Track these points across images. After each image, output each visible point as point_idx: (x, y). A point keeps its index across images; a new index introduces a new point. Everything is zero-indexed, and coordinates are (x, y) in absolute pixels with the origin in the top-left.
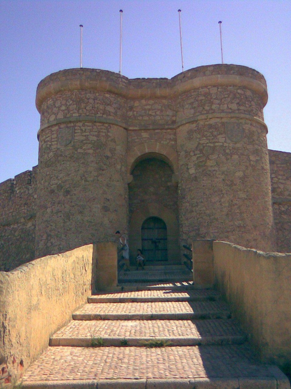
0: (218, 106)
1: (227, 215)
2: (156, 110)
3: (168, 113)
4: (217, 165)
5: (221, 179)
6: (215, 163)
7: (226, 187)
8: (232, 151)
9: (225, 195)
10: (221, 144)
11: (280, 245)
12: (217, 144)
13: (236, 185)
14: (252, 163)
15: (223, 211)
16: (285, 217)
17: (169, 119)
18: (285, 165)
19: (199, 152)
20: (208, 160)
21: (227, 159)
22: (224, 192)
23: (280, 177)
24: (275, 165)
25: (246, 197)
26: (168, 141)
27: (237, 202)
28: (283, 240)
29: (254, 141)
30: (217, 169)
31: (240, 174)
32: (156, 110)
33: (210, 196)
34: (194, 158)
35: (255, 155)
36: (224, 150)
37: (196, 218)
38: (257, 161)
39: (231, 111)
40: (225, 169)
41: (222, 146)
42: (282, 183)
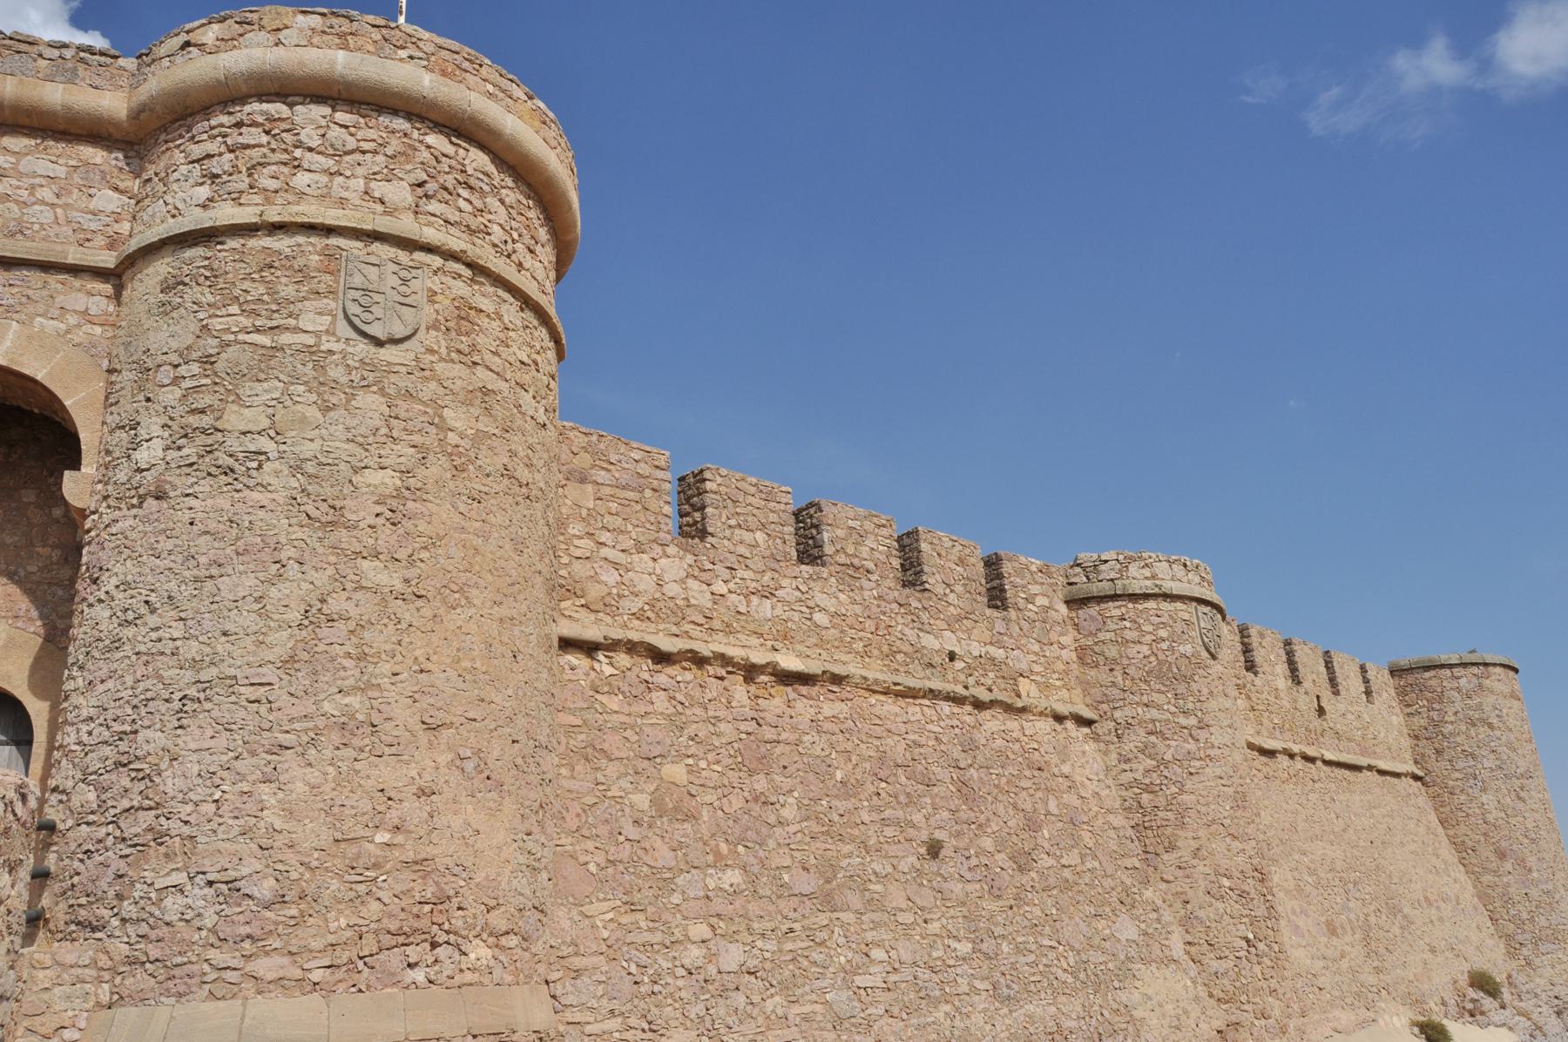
0: (324, 179)
1: (289, 663)
2: (37, 181)
3: (94, 204)
4: (276, 433)
5: (281, 497)
6: (266, 423)
7: (300, 535)
8: (355, 376)
9: (293, 569)
10: (310, 340)
11: (572, 823)
12: (285, 338)
13: (351, 527)
14: (452, 438)
15: (271, 647)
16: (613, 703)
17: (93, 226)
18: (631, 495)
19: (195, 368)
20: (235, 407)
21: (326, 409)
22: (288, 553)
23: (605, 537)
24: (589, 488)
25: (399, 586)
26: (72, 320)
27: (350, 606)
28: (590, 800)
29: (473, 347)
30: (265, 444)
31: (387, 480)
32: (37, 181)
33: (214, 571)
34: (171, 396)
35: (475, 411)
36: (320, 367)
37: (129, 680)
38: (480, 437)
39: (379, 208)
40: (308, 449)
41: (310, 350)
42: (616, 565)
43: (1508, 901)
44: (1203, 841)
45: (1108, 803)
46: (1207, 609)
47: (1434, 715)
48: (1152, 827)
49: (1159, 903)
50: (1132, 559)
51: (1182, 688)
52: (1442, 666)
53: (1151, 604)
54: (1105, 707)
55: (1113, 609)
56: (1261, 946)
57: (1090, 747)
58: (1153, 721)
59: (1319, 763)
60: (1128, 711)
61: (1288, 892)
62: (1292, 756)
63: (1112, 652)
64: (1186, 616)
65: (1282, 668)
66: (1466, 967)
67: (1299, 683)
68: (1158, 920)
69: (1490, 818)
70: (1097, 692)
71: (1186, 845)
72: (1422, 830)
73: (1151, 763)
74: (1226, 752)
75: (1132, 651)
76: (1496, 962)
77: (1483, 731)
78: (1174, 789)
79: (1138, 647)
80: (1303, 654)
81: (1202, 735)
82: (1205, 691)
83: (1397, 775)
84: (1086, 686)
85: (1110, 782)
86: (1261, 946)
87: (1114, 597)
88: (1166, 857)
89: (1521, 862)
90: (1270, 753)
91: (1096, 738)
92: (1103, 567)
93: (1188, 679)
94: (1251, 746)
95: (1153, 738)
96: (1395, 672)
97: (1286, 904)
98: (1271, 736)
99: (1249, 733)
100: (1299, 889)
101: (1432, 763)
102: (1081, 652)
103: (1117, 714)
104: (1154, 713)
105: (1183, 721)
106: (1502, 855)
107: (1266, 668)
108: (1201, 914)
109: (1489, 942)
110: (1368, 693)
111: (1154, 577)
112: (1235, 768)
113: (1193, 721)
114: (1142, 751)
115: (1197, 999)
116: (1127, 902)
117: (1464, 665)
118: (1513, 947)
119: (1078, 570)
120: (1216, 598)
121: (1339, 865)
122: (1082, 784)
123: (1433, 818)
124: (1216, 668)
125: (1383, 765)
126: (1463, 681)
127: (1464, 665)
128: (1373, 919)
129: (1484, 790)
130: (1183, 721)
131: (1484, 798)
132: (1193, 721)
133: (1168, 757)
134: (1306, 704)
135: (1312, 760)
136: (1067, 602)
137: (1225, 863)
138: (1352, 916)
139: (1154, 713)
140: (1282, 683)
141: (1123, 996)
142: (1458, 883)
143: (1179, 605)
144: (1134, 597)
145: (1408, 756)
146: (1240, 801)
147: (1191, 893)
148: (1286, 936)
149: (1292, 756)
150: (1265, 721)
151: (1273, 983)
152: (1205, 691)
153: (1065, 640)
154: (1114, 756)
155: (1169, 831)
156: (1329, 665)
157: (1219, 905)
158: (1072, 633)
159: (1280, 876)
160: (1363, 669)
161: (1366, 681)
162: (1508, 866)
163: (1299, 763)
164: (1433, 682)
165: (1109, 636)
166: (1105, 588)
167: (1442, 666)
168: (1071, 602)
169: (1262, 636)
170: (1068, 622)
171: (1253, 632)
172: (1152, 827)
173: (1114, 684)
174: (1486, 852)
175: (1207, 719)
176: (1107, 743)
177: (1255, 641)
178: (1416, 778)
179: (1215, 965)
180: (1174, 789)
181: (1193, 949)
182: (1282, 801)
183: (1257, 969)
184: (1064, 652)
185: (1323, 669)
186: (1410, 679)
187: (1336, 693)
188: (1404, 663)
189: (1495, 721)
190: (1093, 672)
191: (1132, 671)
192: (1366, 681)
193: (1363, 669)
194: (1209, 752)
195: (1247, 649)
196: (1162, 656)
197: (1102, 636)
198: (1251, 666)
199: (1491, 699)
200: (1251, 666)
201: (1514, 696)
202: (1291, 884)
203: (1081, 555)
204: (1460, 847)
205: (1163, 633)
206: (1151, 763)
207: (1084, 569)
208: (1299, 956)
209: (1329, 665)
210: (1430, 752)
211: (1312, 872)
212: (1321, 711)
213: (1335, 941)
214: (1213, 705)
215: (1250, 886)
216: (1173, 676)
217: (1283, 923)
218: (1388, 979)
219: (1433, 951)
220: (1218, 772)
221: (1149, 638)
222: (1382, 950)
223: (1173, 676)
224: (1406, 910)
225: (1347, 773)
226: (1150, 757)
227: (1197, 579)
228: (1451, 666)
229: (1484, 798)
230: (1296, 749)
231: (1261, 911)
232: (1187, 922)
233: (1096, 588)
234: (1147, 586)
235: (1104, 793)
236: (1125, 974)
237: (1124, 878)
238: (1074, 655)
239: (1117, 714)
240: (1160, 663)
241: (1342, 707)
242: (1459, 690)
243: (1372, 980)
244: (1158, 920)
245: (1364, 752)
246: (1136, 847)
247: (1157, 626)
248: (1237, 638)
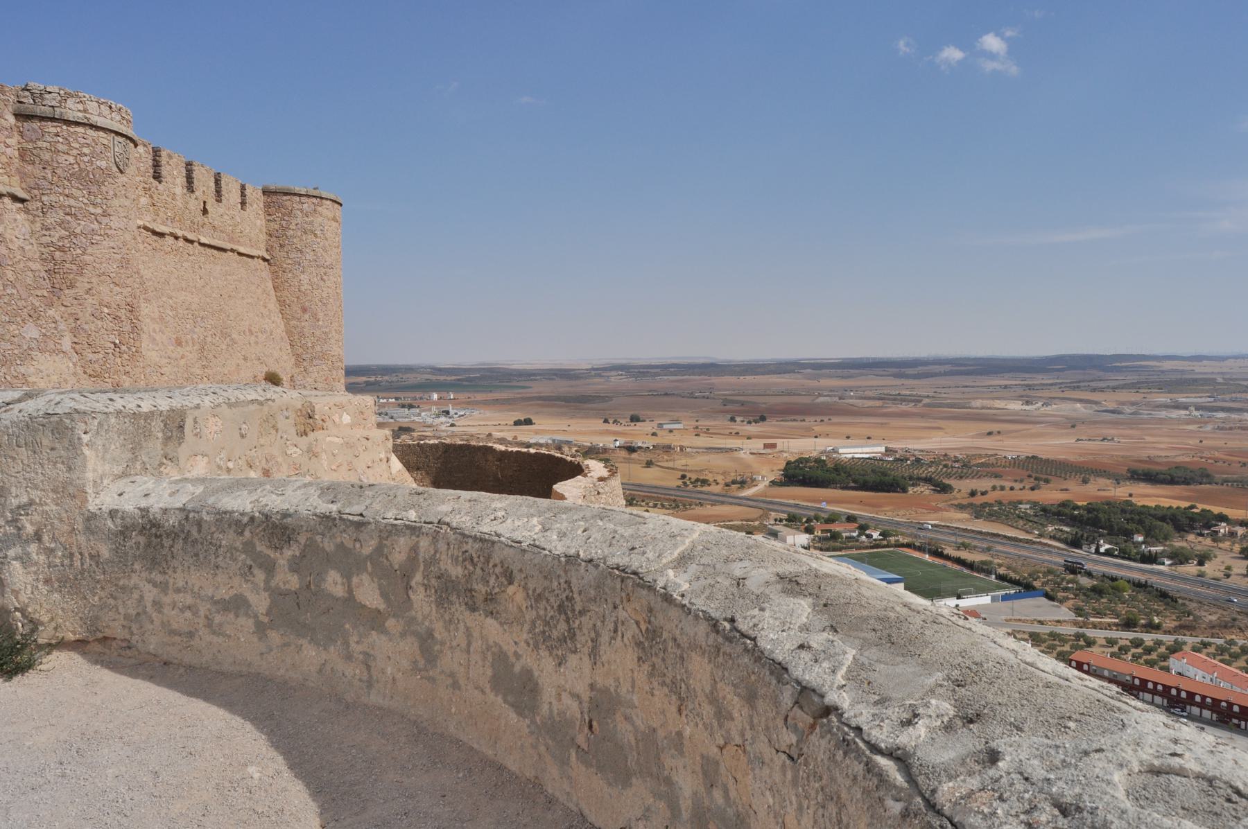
43: (302, 335)
44: (95, 285)
45: (29, 255)
46: (121, 139)
47: (284, 223)
48: (59, 272)
49: (58, 318)
50: (71, 96)
51: (94, 189)
52: (295, 194)
53: (80, 129)
54: (36, 192)
55: (51, 128)
56: (124, 348)
57: (21, 217)
58: (70, 207)
59: (196, 244)
60: (53, 198)
61: (153, 319)
62: (176, 238)
63: (47, 156)
64: (105, 142)
65: (181, 180)
66: (266, 369)
67: (193, 191)
68: (56, 328)
69: (303, 289)
70: (31, 181)
71: (82, 285)
72: (259, 291)
73: (64, 233)
74: (120, 233)
75: (62, 158)
76: (285, 367)
77: (310, 237)
78: (79, 251)
79: (66, 157)
80: (198, 173)
81: (105, 220)
82: (111, 193)
83: (252, 257)
84: (23, 176)
85: (33, 241)
86: (124, 348)
87: (53, 119)
88: (67, 291)
89: (315, 317)
90: (161, 235)
91: (27, 211)
92: (47, 96)
93: (99, 184)
94: (146, 228)
95: (69, 218)
96: (266, 192)
97: (147, 325)
98: (164, 223)
99: (147, 220)
100: (161, 318)
101: (277, 253)
102: (23, 153)
103: (44, 198)
104: (72, 202)
105: (92, 209)
106: (304, 310)
107: (169, 179)
108: (86, 327)
109: (285, 357)
110: (243, 203)
111: (85, 111)
112: (124, 244)
113: (99, 211)
114: (60, 225)
115: (75, 374)
116: (35, 315)
117: (309, 196)
118: (299, 361)
119: (27, 93)
120: (130, 133)
121: (194, 306)
122: (11, 241)
123: (270, 285)
124: (122, 179)
125: (242, 250)
126: (305, 206)
127: (309, 196)
128: (209, 339)
129: (303, 272)
130: (92, 209)
131: (302, 277)
132: (99, 211)
133: (78, 231)
134: (194, 205)
135: (192, 242)
136: (15, 115)
137: (107, 299)
138: (195, 336)
139: (72, 202)
140: (179, 190)
141: (22, 369)
142: (277, 325)
143: (101, 134)
144: (68, 123)
145: (263, 246)
146: (125, 263)
147: (81, 314)
148: (145, 344)
149: (176, 238)
150: (161, 214)
151: (128, 369)
152: (111, 193)
153: (12, 141)
154: (38, 225)
155: (71, 276)
156: (218, 182)
157: (99, 323)
158: (17, 138)
159: (145, 310)
160: (243, 187)
161: (243, 195)
162: (307, 317)
163: (181, 243)
164: (287, 203)
165: (45, 145)
166: (47, 111)
167: (295, 194)
168: (22, 116)
169: (170, 157)
170: (15, 129)
171: (164, 154)
172: (59, 272)
173: (45, 178)
174: (296, 308)
175: (110, 211)
176: (35, 216)
177: (164, 159)
178: (264, 260)
179: (91, 356)
180: (79, 251)
181: (77, 347)
182: (156, 265)
183: (118, 360)
184: (8, 150)
185: (212, 184)
186: (274, 198)
187: (219, 201)
188: (272, 187)
189: (318, 233)
190: (30, 168)
191: (59, 171)
192: (243, 195)
193: (243, 187)
194: (109, 232)
195: (156, 165)
196: (82, 166)
197: (40, 144)
198: (157, 176)
199: (320, 219)
200: (157, 176)
201: (334, 219)
202: (157, 315)
203: (31, 84)
204: (282, 303)
205: (86, 150)
206: (64, 233)
207: (32, 94)
208: (151, 354)
209: (218, 182)
210: (277, 246)
211: (173, 309)
212: (205, 211)
213: (179, 349)
214: (116, 202)
215: (122, 314)
216: (89, 180)
217: (144, 336)
218: (210, 372)
219: (245, 359)
220: (112, 244)
221: (75, 152)
222: (210, 356)
223: (89, 180)
224: (234, 336)
225: (216, 252)
226: (64, 229)
227: (119, 118)
228: (300, 195)
229: (302, 277)
230: (180, 233)
231: (128, 328)
232: (75, 331)
233: (40, 110)
234: (79, 116)
235: (27, 248)
236: (26, 356)
237: (34, 302)
238: (16, 153)
239: (44, 198)
240: (81, 170)
241: (221, 210)
242: (302, 210)
243: (198, 372)
244: (56, 328)
245: (231, 240)
246: (47, 284)
247: (82, 145)
248: (150, 157)
